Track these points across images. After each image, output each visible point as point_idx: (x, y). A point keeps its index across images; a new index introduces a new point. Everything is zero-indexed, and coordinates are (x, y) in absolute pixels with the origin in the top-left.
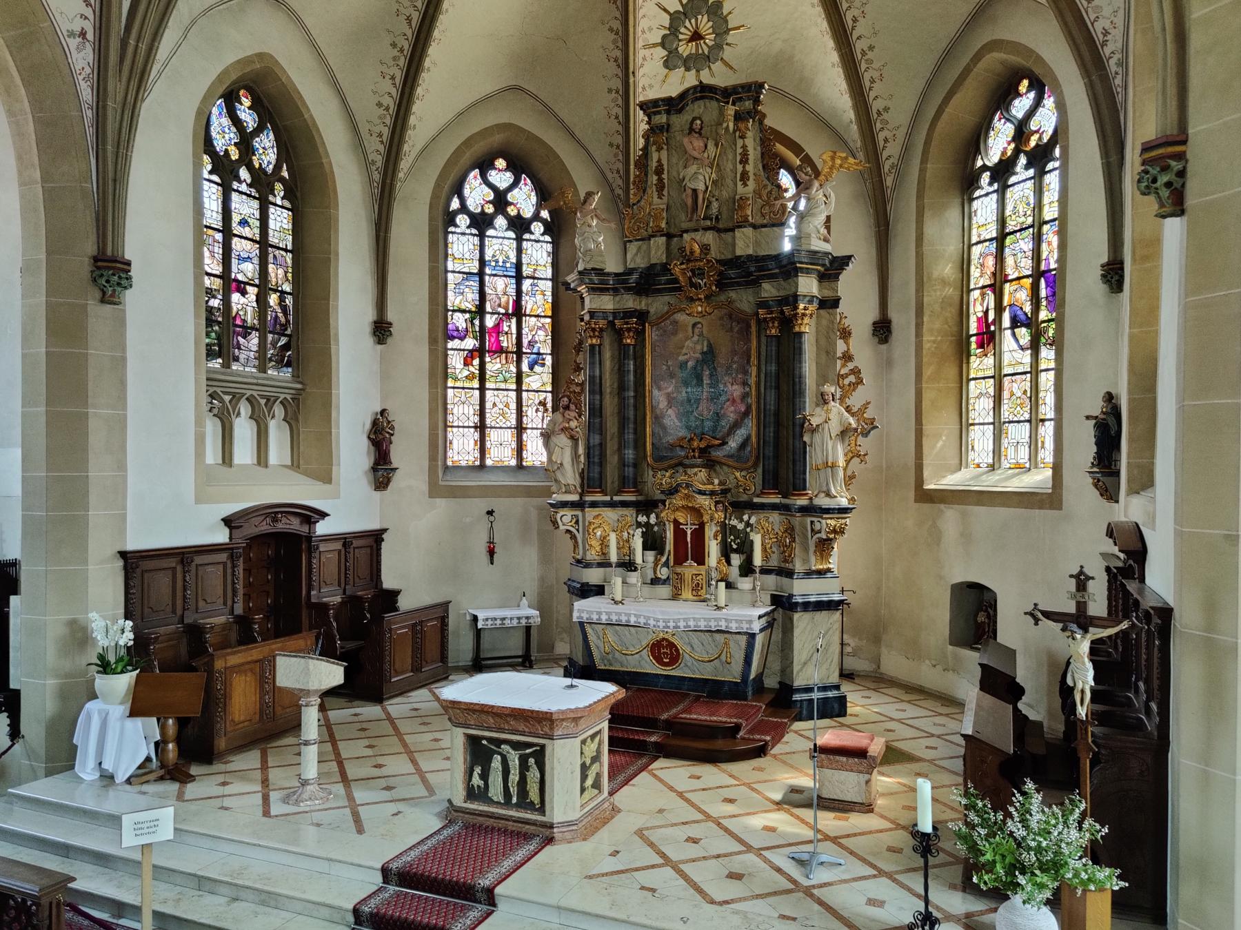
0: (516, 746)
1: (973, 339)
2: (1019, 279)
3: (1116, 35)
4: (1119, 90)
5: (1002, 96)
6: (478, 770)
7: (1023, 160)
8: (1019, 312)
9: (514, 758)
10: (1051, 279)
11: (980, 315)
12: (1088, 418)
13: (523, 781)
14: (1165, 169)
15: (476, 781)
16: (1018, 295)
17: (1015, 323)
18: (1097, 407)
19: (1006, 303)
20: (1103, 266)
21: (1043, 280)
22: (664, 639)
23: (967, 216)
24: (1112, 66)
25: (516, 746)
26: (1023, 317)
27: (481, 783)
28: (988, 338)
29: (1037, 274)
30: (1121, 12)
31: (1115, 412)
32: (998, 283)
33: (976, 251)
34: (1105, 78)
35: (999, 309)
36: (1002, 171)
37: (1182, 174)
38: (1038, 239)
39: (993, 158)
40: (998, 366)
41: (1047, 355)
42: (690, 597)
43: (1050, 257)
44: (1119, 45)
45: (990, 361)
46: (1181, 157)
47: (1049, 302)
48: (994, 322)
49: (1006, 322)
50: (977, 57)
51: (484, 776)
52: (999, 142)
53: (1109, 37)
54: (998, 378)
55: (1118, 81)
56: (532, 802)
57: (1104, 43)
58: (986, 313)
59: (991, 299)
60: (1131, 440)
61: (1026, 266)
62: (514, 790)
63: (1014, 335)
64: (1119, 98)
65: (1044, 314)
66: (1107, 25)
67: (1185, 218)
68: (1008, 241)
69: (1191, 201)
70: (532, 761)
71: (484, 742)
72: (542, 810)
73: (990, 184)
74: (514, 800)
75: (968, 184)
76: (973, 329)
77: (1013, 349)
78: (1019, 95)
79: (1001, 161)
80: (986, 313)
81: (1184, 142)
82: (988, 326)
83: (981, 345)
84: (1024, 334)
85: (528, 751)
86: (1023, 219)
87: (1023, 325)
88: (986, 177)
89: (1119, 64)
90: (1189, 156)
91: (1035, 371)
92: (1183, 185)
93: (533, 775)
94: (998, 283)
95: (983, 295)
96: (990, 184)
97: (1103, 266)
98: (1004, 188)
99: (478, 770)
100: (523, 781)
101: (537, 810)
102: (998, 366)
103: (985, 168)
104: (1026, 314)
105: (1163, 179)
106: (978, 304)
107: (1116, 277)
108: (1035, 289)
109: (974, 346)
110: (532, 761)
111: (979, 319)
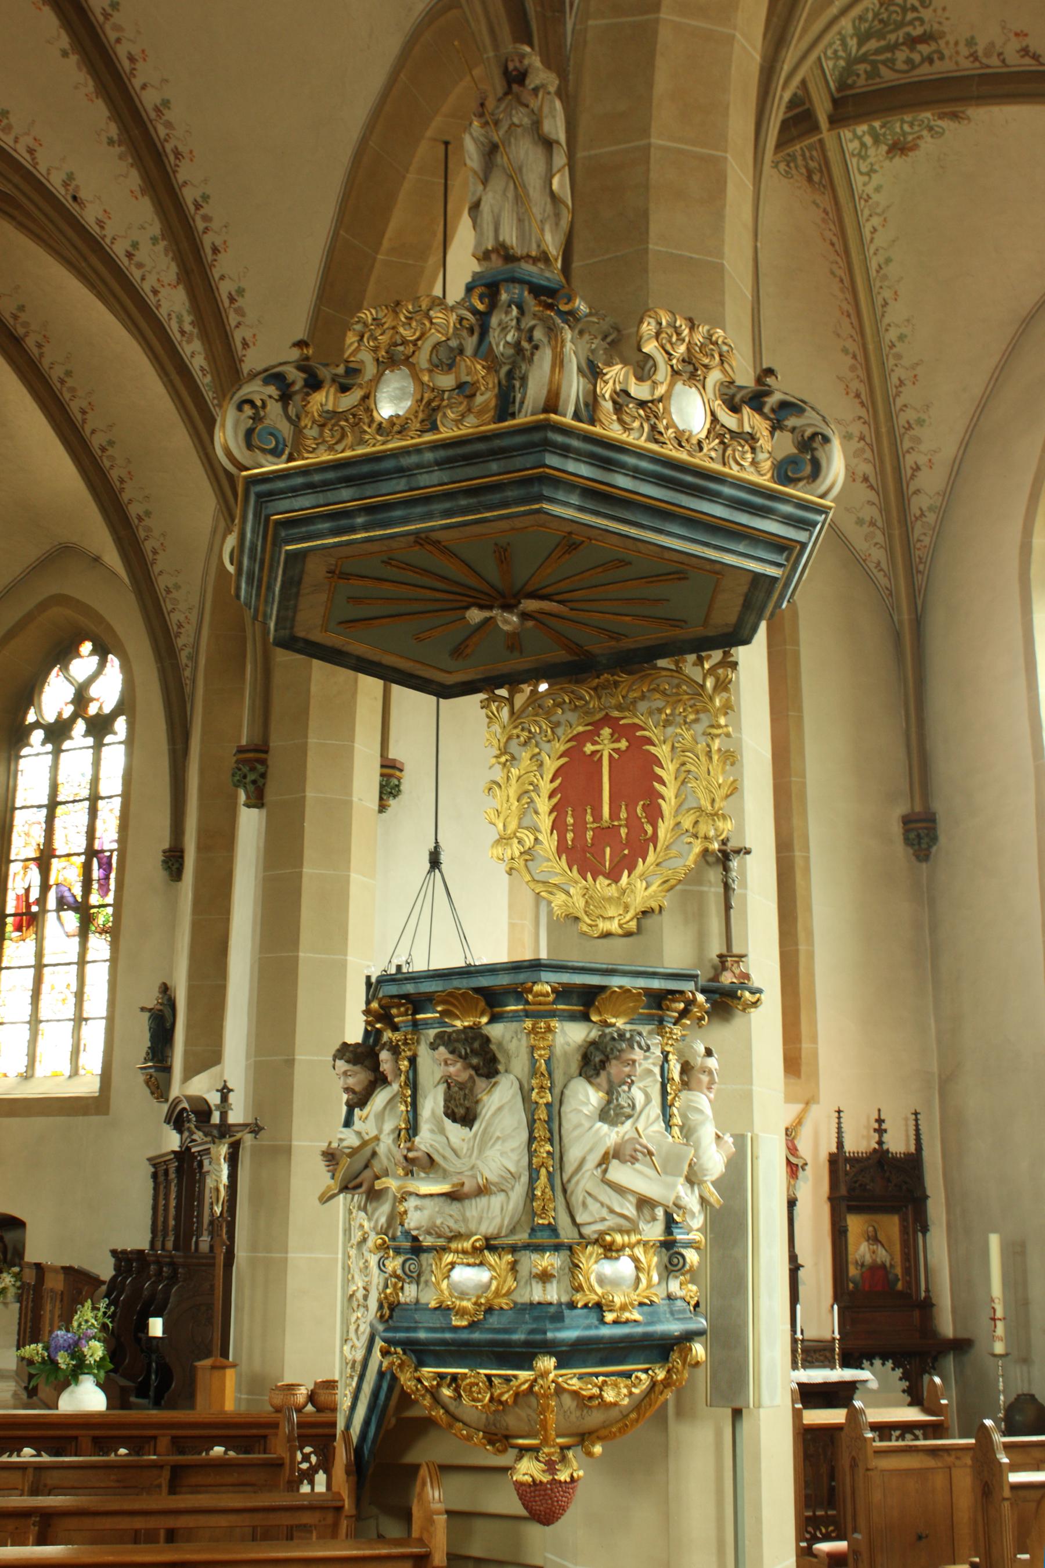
1: (10, 920)
2: (69, 855)
3: (189, 630)
4: (188, 682)
5: (62, 654)
7: (80, 726)
8: (67, 894)
10: (105, 860)
11: (22, 892)
12: (143, 1009)
14: (253, 769)
16: (67, 873)
17: (62, 904)
18: (152, 999)
19: (51, 882)
20: (164, 852)
21: (95, 861)
23: (11, 774)
24: (183, 657)
26: (70, 899)
28: (30, 919)
29: (91, 852)
30: (195, 612)
31: (172, 1005)
32: (44, 859)
33: (19, 817)
34: (177, 668)
35: (45, 887)
36: (57, 733)
37: (263, 775)
38: (93, 813)
39: (50, 717)
40: (39, 954)
41: (99, 947)
43: (108, 837)
44: (191, 640)
45: (30, 945)
46: (263, 762)
47: (101, 886)
48: (38, 902)
49: (51, 902)
50: (43, 606)
52: (55, 697)
53: (182, 630)
54: (39, 967)
55: (187, 673)
57: (178, 635)
58: (27, 890)
59: (34, 875)
60: (189, 1026)
61: (81, 845)
63: (59, 918)
64: (188, 690)
65: (95, 899)
66: (182, 619)
67: (264, 811)
68: (60, 810)
69: (270, 797)
73: (43, 743)
75: (19, 736)
76: (10, 908)
77: (60, 931)
78: (79, 656)
79: (57, 721)
80: (27, 890)
81: (266, 752)
82: (28, 906)
83: (18, 928)
84: (71, 919)
86: (76, 790)
87: (70, 908)
88: (38, 735)
89: (190, 657)
90: (270, 763)
91: (82, 962)
92: (264, 785)
94: (44, 859)
95: (26, 868)
96: (43, 743)
97: (164, 852)
98: (57, 752)
102: (39, 954)
103: (37, 725)
104: (74, 896)
105: (251, 777)
106: (19, 878)
107: (176, 866)
108: (87, 868)
109: (9, 928)
111: (18, 897)
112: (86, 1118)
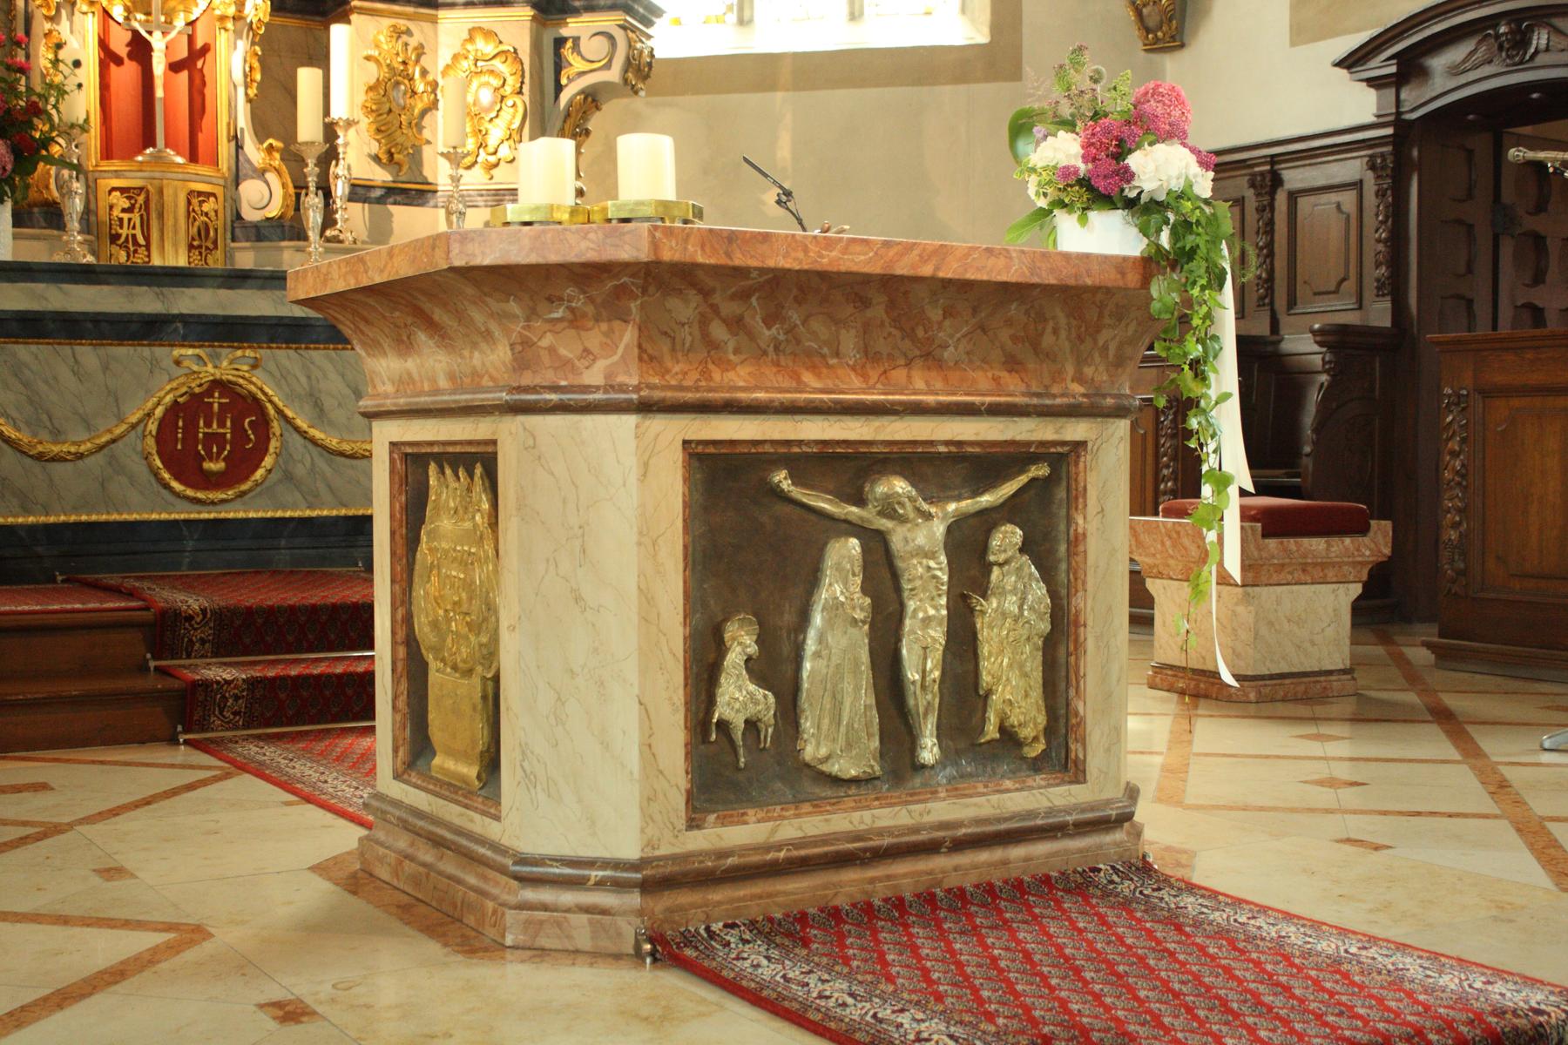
0: (933, 468)
6: (741, 642)
9: (923, 538)
13: (962, 640)
15: (739, 696)
22: (217, 384)
25: (933, 468)
27: (762, 702)
42: (219, 253)
51: (778, 669)
56: (1009, 736)
62: (925, 699)
70: (1007, 538)
71: (782, 479)
72: (1060, 751)
74: (929, 751)
85: (987, 499)
93: (1014, 602)
99: (741, 642)
100: (962, 640)
101: (1036, 765)
110: (1007, 538)
112: (962, 88)
